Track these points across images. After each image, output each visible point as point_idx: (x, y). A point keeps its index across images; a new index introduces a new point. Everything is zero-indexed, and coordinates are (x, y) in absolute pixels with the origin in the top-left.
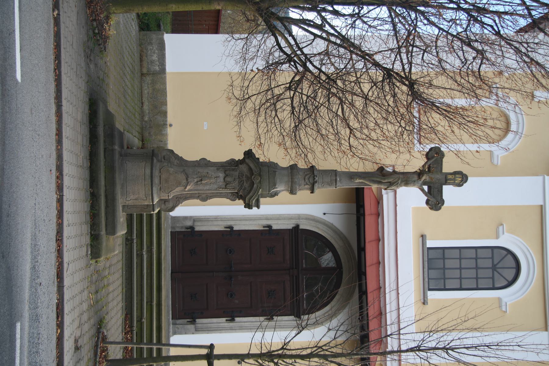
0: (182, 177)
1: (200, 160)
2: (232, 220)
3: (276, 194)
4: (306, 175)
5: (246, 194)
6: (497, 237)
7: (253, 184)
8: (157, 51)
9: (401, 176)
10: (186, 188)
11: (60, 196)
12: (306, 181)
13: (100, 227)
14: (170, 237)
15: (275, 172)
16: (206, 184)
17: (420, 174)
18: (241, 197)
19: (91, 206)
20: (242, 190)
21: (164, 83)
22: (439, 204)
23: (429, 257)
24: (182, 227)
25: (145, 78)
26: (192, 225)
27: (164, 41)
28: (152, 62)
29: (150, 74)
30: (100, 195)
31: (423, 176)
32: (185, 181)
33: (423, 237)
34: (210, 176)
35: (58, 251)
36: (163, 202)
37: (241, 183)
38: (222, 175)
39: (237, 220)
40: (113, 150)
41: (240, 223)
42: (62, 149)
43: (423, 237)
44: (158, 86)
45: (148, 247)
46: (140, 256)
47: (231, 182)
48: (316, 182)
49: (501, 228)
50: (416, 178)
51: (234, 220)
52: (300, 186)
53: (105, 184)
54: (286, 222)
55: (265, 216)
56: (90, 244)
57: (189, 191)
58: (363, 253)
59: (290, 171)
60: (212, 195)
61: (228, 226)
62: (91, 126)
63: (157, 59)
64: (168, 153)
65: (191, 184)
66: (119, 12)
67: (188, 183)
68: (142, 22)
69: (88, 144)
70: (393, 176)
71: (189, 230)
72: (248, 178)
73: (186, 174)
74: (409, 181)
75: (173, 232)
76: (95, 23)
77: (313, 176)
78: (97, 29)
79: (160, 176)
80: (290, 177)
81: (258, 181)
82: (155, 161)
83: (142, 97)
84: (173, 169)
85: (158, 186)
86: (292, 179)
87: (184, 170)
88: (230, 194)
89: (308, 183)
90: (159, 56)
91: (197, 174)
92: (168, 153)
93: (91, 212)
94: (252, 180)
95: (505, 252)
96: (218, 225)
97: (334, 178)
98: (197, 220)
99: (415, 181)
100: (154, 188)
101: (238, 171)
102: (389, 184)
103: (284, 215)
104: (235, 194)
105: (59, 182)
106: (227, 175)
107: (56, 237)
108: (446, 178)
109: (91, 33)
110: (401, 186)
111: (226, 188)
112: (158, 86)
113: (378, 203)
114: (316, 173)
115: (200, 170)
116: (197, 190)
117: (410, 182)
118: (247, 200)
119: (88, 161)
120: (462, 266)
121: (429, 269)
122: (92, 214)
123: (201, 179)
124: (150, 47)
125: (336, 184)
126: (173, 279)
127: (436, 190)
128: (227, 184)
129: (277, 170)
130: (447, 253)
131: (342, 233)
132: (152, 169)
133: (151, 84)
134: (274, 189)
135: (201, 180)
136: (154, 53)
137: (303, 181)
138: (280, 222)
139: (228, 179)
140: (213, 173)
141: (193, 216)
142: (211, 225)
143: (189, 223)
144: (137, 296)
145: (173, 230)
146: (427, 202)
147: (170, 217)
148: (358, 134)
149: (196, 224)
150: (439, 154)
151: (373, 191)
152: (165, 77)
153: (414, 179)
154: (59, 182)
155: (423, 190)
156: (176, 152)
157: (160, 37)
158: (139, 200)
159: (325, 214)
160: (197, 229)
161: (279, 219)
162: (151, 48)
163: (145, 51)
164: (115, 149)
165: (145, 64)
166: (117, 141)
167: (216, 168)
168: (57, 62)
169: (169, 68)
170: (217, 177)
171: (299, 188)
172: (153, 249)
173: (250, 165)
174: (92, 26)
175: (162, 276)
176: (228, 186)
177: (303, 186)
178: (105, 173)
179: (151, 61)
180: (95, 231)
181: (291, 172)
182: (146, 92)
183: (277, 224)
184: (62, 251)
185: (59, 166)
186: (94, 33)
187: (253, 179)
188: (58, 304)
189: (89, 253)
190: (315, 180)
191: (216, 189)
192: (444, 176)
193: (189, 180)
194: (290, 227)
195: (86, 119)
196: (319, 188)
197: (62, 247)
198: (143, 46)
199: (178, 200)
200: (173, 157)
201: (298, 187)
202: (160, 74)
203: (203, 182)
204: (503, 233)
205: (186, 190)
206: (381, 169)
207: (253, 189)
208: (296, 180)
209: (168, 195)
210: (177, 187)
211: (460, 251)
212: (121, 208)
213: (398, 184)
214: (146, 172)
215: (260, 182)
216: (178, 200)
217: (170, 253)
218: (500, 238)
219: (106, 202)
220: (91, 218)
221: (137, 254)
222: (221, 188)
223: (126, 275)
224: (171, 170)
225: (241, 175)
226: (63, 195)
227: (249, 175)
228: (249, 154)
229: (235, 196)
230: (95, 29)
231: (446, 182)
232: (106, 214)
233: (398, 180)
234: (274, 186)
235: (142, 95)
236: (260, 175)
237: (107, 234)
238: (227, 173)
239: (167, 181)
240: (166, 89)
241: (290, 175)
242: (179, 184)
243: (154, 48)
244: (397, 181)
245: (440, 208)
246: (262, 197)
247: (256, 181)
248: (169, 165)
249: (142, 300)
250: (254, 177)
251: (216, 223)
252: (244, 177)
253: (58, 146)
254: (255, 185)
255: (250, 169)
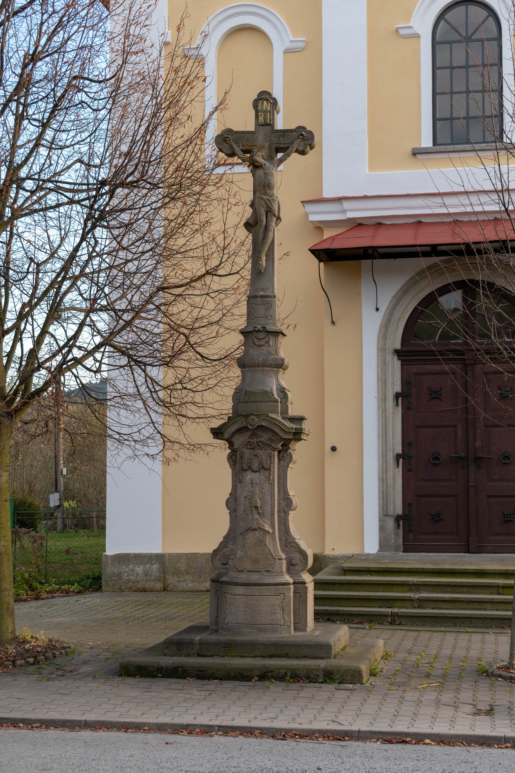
0: (251, 537)
1: (228, 508)
2: (386, 456)
3: (283, 391)
4: (254, 343)
5: (278, 438)
6: (417, 36)
7: (261, 426)
8: (131, 567)
9: (258, 195)
10: (268, 532)
11: (219, 730)
12: (262, 343)
13: (313, 667)
14: (411, 554)
15: (246, 392)
16: (263, 500)
17: (255, 166)
18: (286, 445)
19: (280, 681)
20: (273, 445)
21: (178, 556)
22: (302, 135)
23: (449, 142)
24: (397, 534)
25: (170, 586)
26: (393, 519)
27: (116, 555)
28: (146, 574)
29: (164, 578)
30: (264, 666)
31: (257, 162)
32: (257, 533)
33: (416, 153)
34: (250, 494)
35: (301, 737)
36: (292, 567)
37: (261, 445)
38: (249, 476)
39: (386, 447)
40: (201, 643)
41: (391, 442)
42: (148, 724)
43: (416, 153)
44: (182, 567)
45: (411, 590)
46: (421, 603)
47: (260, 462)
48: (264, 328)
49: (402, 32)
50: (260, 172)
51: (386, 451)
52: (270, 353)
53: (252, 657)
54: (390, 369)
55: (380, 404)
56: (337, 685)
57: (273, 526)
58: (439, 248)
59: (248, 369)
60: (282, 492)
61: (396, 462)
62: (160, 675)
63: (141, 567)
64: (218, 558)
65: (263, 523)
66: (11, 625)
67: (260, 528)
68: (90, 587)
69: (185, 681)
70: (257, 208)
71: (401, 523)
72: (254, 435)
73: (246, 531)
74: (265, 182)
75: (404, 548)
76: (19, 662)
77: (255, 333)
78: (28, 660)
79: (248, 571)
80: (257, 368)
81: (256, 419)
82: (225, 579)
83: (198, 591)
84: (239, 552)
85: (263, 574)
86: (259, 366)
87: (242, 534)
88: (282, 462)
89: (266, 340)
90: (137, 563)
91: (247, 515)
92: (218, 558)
93: (289, 682)
94: (256, 428)
95: (442, 23)
96: (394, 478)
97: (260, 299)
98: (385, 510)
99: (266, 173)
100: (266, 581)
101: (243, 449)
102: (269, 214)
103: (378, 374)
104: (281, 455)
105: (198, 730)
106: (250, 467)
107: (278, 739)
108: (263, 125)
109: (31, 669)
110: (273, 194)
111: (269, 469)
112: (182, 567)
113: (360, 225)
114: (250, 329)
115: (241, 509)
116: (273, 515)
117: (266, 181)
118: (286, 437)
119: (211, 681)
120: (464, 89)
121: (468, 142)
122: (292, 680)
123: (254, 509)
124: (125, 576)
125: (269, 297)
126: (478, 551)
127: (282, 139)
128: (265, 468)
129: (244, 390)
130: (444, 112)
131: (408, 281)
132: (237, 584)
133: (179, 577)
134: (273, 395)
135: (256, 507)
136: (133, 570)
137: (263, 348)
138: (390, 380)
139: (255, 465)
140: (247, 489)
141: (379, 516)
142: (394, 489)
143: (390, 523)
144: (485, 610)
145: (402, 549)
146: (303, 153)
147: (380, 553)
148: (214, 262)
149: (391, 512)
150: (227, 138)
151: (339, 235)
152: (169, 555)
153: (262, 175)
154: (198, 730)
155: (281, 161)
156: (215, 547)
157: (109, 561)
158: (284, 604)
159: (377, 309)
160: (399, 511)
161: (385, 380)
162: (125, 575)
163: (130, 584)
164: (200, 640)
165: (149, 585)
166: (187, 637)
167: (239, 485)
168: (21, 725)
169: (157, 549)
170: (252, 483)
171: (274, 355)
172: (413, 581)
173: (233, 431)
174: (22, 666)
175: (469, 570)
176: (265, 467)
177: (270, 348)
178: (235, 656)
179: (146, 575)
180: (318, 676)
181: (249, 367)
182: (190, 585)
183: (393, 384)
184: (304, 730)
185: (174, 730)
186: (34, 664)
187: (253, 426)
188: (385, 741)
189: (351, 686)
190: (261, 329)
191: (272, 485)
192: (261, 127)
193: (255, 526)
194: (398, 364)
195: (144, 683)
196: (274, 324)
197: (298, 730)
198: (123, 587)
199: (290, 543)
200: (224, 550)
201: (272, 357)
202: (164, 562)
203: (259, 505)
204: (411, 27)
205: (271, 531)
206: (248, 226)
207: (269, 426)
208: (261, 359)
209: (279, 559)
210: (265, 545)
211: (439, 94)
212: (299, 634)
213: (268, 200)
214: (240, 593)
215: (258, 416)
216: (290, 543)
217: (437, 554)
218: (419, 32)
219: (280, 656)
220: (298, 681)
221: (419, 607)
222: (269, 477)
223: (449, 626)
224: (239, 553)
225: (248, 445)
226: (219, 726)
227: (249, 433)
228: (217, 433)
229: (285, 455)
230: (28, 662)
231: (270, 125)
232: (298, 657)
233: (263, 199)
234: (268, 394)
235: (195, 591)
236: (247, 416)
237: (329, 657)
238: (246, 467)
239: (256, 561)
240: (186, 554)
241: (252, 369)
242: (261, 543)
243: (127, 570)
244: (265, 201)
245: (310, 132)
246: (287, 413)
247: (257, 422)
248: (232, 557)
249: (492, 602)
250: (251, 424)
251: (390, 482)
252: (252, 441)
253: (144, 730)
254: (263, 424)
255: (240, 431)
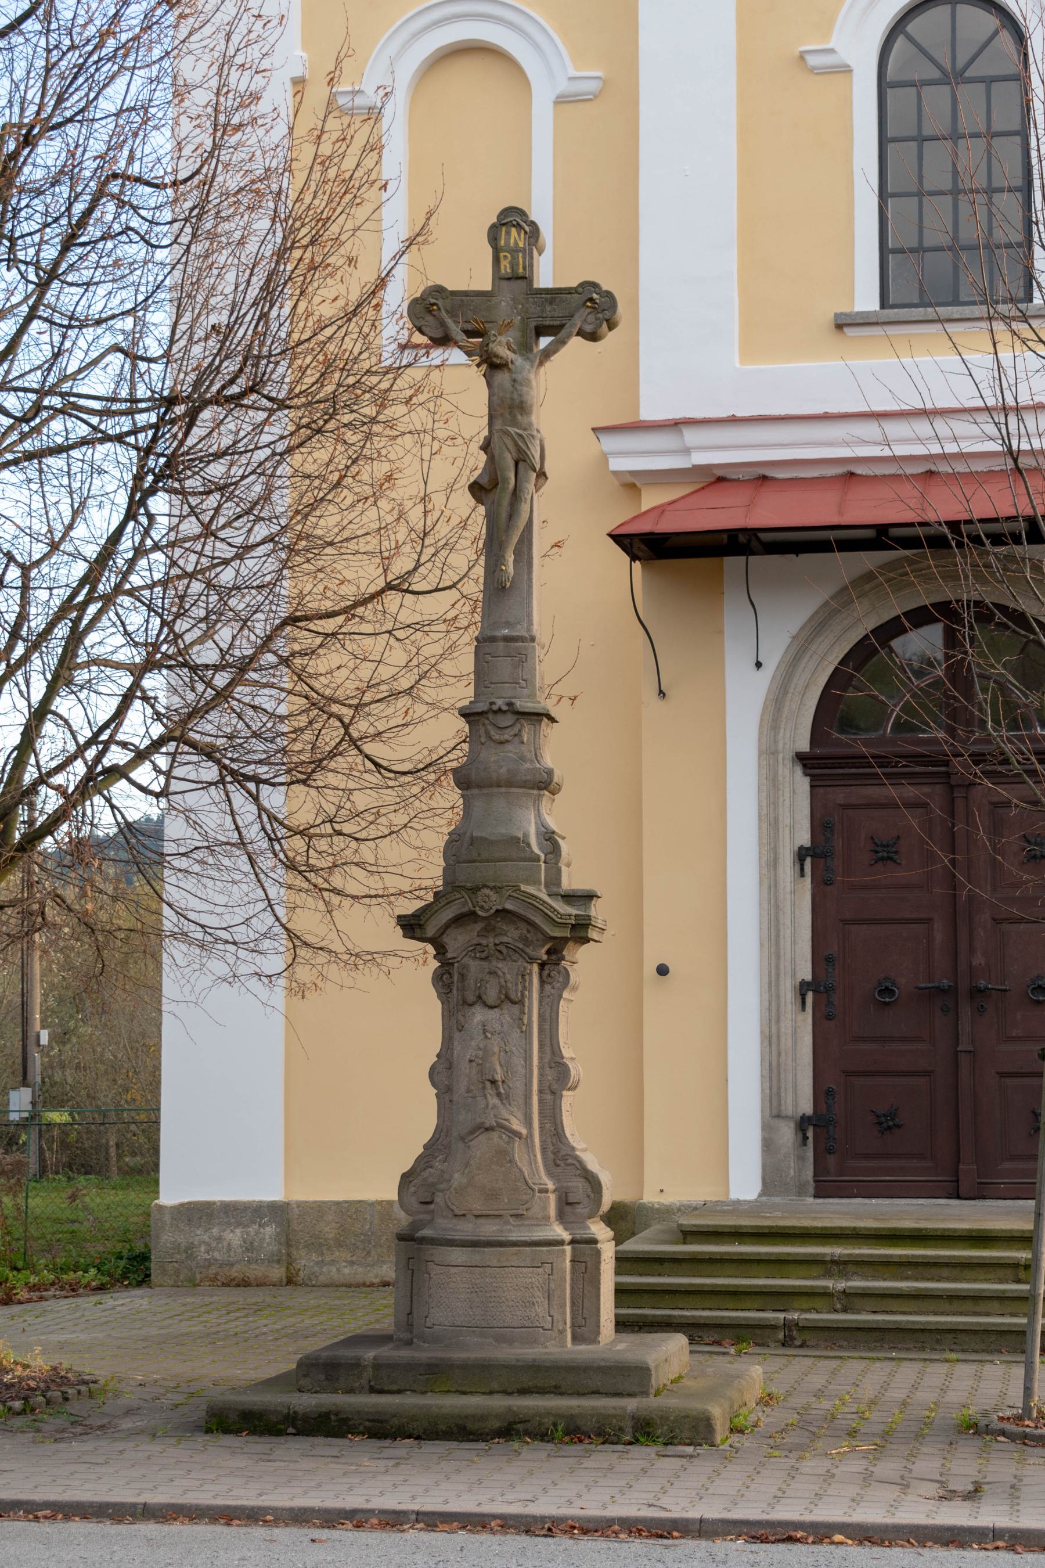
0: (483, 1145)
2: (778, 986)
3: (550, 839)
4: (490, 737)
5: (540, 936)
6: (845, 70)
8: (215, 1231)
9: (498, 426)
11: (417, 1521)
12: (506, 737)
13: (612, 1412)
14: (831, 1200)
15: (473, 840)
16: (507, 1066)
17: (492, 365)
18: (556, 952)
19: (542, 1440)
20: (528, 950)
21: (320, 1208)
22: (591, 300)
23: (916, 301)
24: (801, 1158)
25: (301, 1274)
26: (792, 1125)
27: (182, 1205)
28: (249, 1247)
29: (289, 1255)
30: (509, 1409)
31: (497, 356)
32: (495, 1135)
33: (842, 324)
34: (480, 1052)
35: (585, 1532)
36: (568, 1209)
37: (504, 951)
38: (479, 1015)
39: (777, 968)
40: (377, 1366)
41: (788, 956)
42: (274, 1510)
43: (842, 324)
44: (329, 1231)
45: (828, 1274)
46: (850, 1299)
47: (501, 986)
48: (510, 704)
49: (813, 61)
50: (502, 378)
51: (778, 975)
52: (523, 758)
53: (484, 1393)
54: (787, 795)
55: (765, 871)
56: (660, 1448)
57: (528, 1122)
58: (894, 532)
59: (475, 791)
60: (548, 1050)
61: (799, 1000)
62: (291, 1430)
63: (238, 1231)
65: (507, 1116)
67: (501, 1126)
68: (124, 1276)
70: (496, 453)
71: (810, 1134)
72: (489, 929)
74: (512, 399)
75: (816, 1188)
77: (491, 716)
78: (10, 1404)
79: (477, 1216)
80: (495, 790)
81: (494, 897)
82: (427, 1232)
83: (364, 1285)
84: (456, 1175)
85: (507, 1223)
86: (499, 786)
87: (462, 1139)
88: (548, 987)
90: (229, 1224)
91: (474, 1097)
92: (412, 1189)
93: (561, 1442)
95: (900, 42)
96: (795, 1033)
97: (501, 644)
98: (775, 1104)
99: (514, 381)
100: (514, 1237)
101: (466, 960)
102: (521, 465)
103: (760, 806)
104: (546, 973)
105: (375, 1521)
106: (480, 997)
107: (537, 1536)
108: (509, 279)
109: (18, 1422)
110: (530, 424)
111: (520, 1002)
112: (329, 1231)
113: (721, 480)
116: (528, 1097)
117: (516, 397)
118: (557, 933)
119: (399, 1442)
120: (948, 186)
121: (956, 302)
122: (567, 1439)
123: (488, 1084)
124: (202, 1252)
125: (522, 639)
126: (979, 1194)
127: (548, 308)
129: (468, 835)
130: (901, 237)
131: (826, 604)
132: (451, 1243)
133: (322, 1254)
134: (529, 845)
135: (493, 1082)
136: (219, 1239)
137: (509, 747)
138: (785, 819)
139: (492, 994)
140: (473, 1043)
141: (763, 1117)
142: (794, 1060)
143: (787, 1133)
144: (988, 1314)
145: (811, 1190)
146: (593, 337)
147: (764, 1199)
148: (401, 565)
149: (788, 1109)
150: (433, 305)
151: (673, 502)
152: (300, 1204)
153: (508, 384)
155: (547, 354)
157: (167, 1218)
158: (552, 1286)
159: (759, 665)
160: (806, 1106)
161: (776, 820)
162: (203, 1248)
163: (212, 1271)
164: (375, 1358)
165: (255, 1271)
166: (350, 1353)
167: (457, 1035)
169: (274, 1193)
170: (485, 1031)
171: (531, 761)
172: (833, 1255)
173: (444, 921)
175: (955, 1230)
176: (513, 996)
177: (523, 748)
178: (449, 1391)
179: (247, 1250)
180: (621, 1429)
181: (479, 787)
182: (346, 1271)
183: (792, 829)
184: (589, 1520)
185: (326, 1522)
186: (23, 1412)
187: (487, 911)
188: (753, 1537)
189: (690, 1449)
190: (504, 708)
191: (527, 1035)
192: (505, 283)
193: (491, 1121)
194: (803, 784)
195: (261, 1444)
196: (532, 696)
197: (579, 1519)
198: (198, 1276)
199: (564, 1159)
200: (426, 1174)
201: (528, 765)
202: (288, 1221)
203: (499, 1077)
204: (831, 51)
205: (524, 1131)
206: (477, 489)
207: (522, 912)
208: (503, 770)
209: (541, 1191)
211: (894, 195)
212: (582, 1347)
213: (520, 435)
214: (459, 1261)
215: (496, 889)
217: (888, 1201)
218: (849, 63)
219: (542, 1391)
220: (581, 1441)
221: (845, 1310)
222: (521, 1019)
223: (908, 1349)
225: (477, 950)
226: (418, 1513)
227: (479, 926)
229: (553, 973)
230: (10, 1409)
231: (524, 278)
232: (579, 1394)
233: (507, 434)
234: (518, 843)
235: (358, 1286)
236: (475, 890)
237: (645, 1393)
238: (471, 998)
239: (493, 1195)
240: (338, 1203)
241: (485, 791)
242: (504, 1156)
243: (206, 1238)
245: (609, 295)
246: (559, 884)
247: (494, 901)
248: (442, 1186)
249: (1002, 1298)
250: (482, 907)
251: (787, 1042)
252: (484, 942)
253: (265, 1521)
254: (509, 906)
255: (461, 920)
